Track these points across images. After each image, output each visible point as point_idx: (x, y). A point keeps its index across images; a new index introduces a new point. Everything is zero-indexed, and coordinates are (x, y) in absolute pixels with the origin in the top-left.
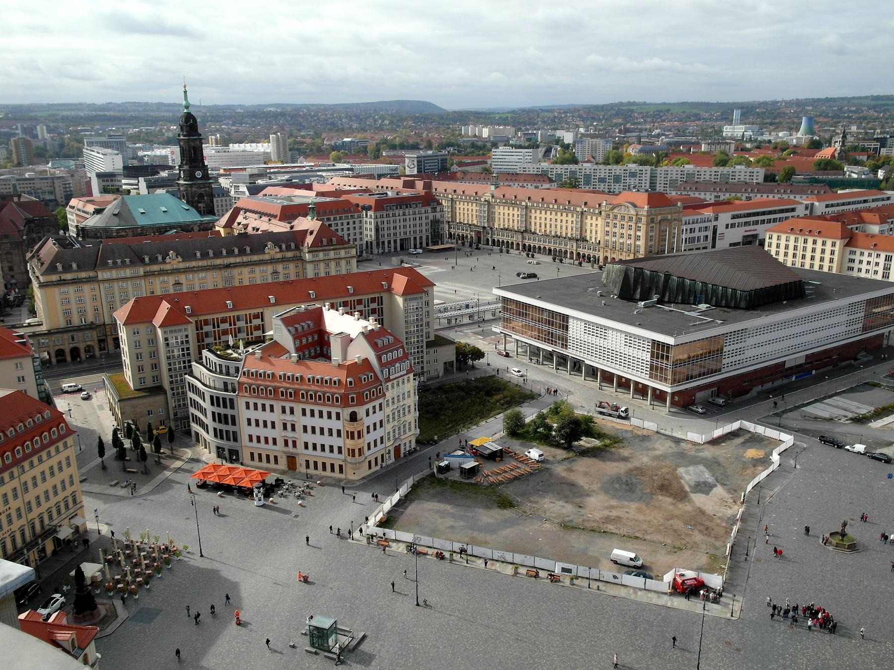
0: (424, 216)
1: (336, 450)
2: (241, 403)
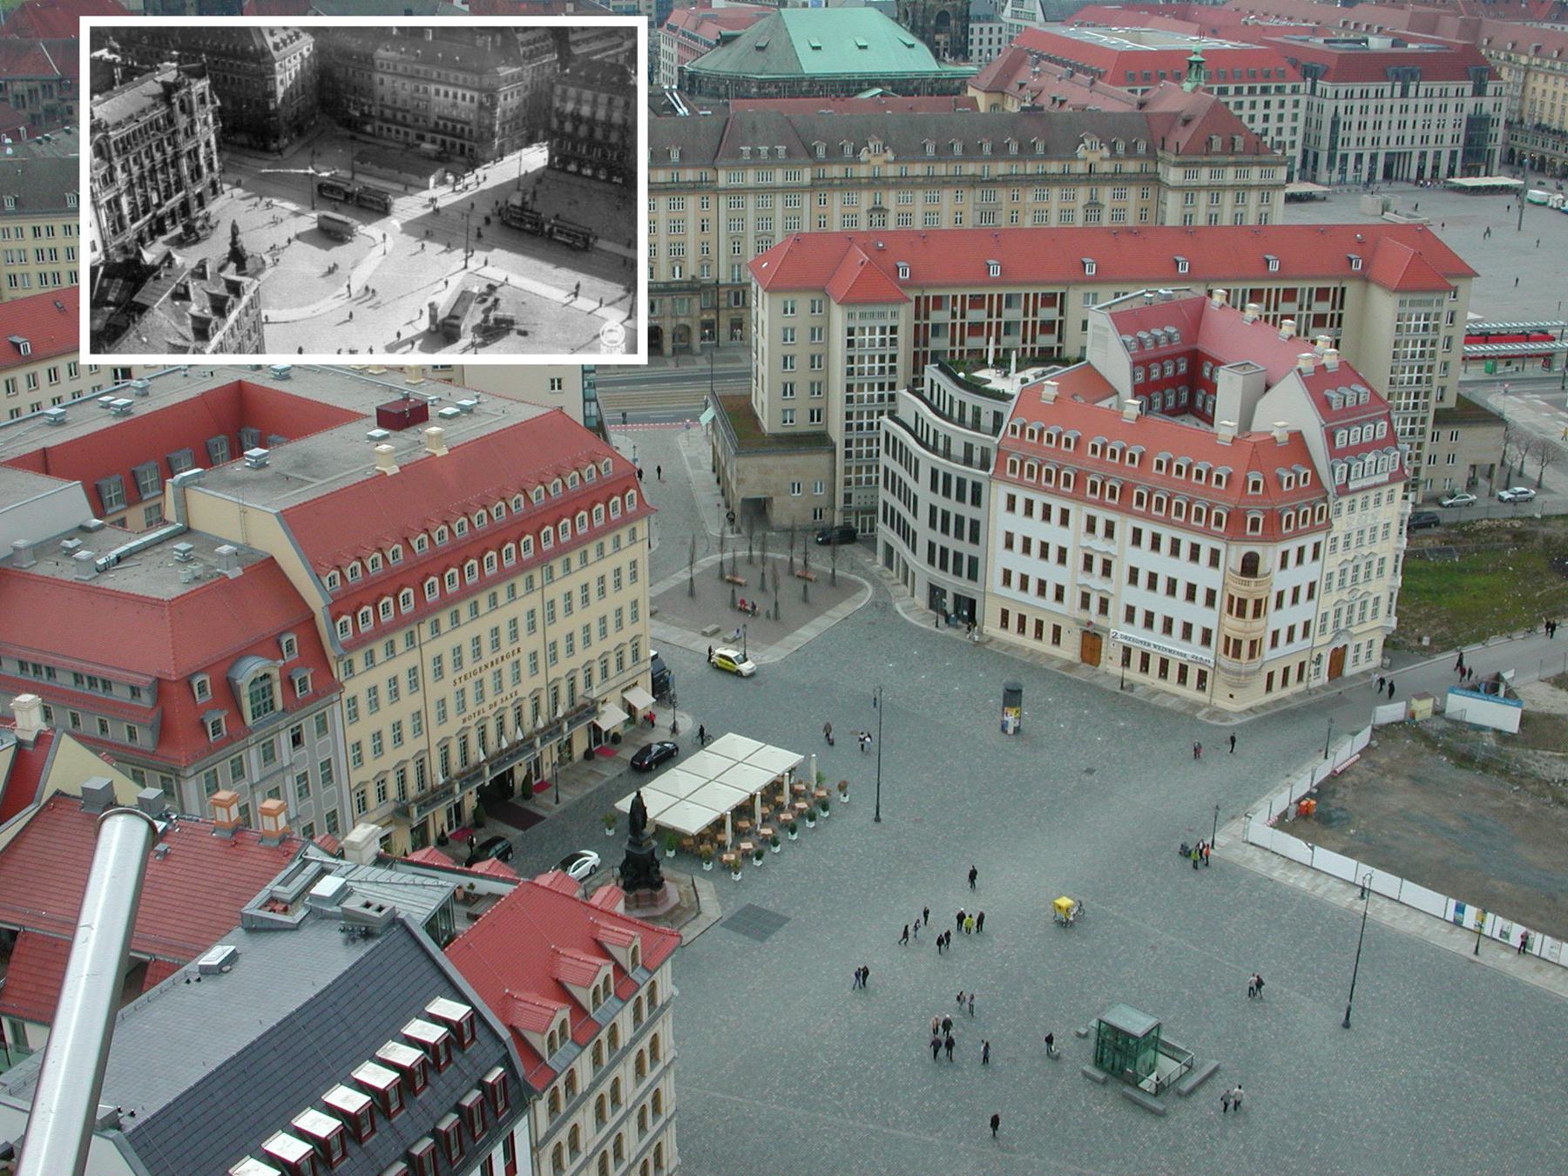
2: (997, 494)
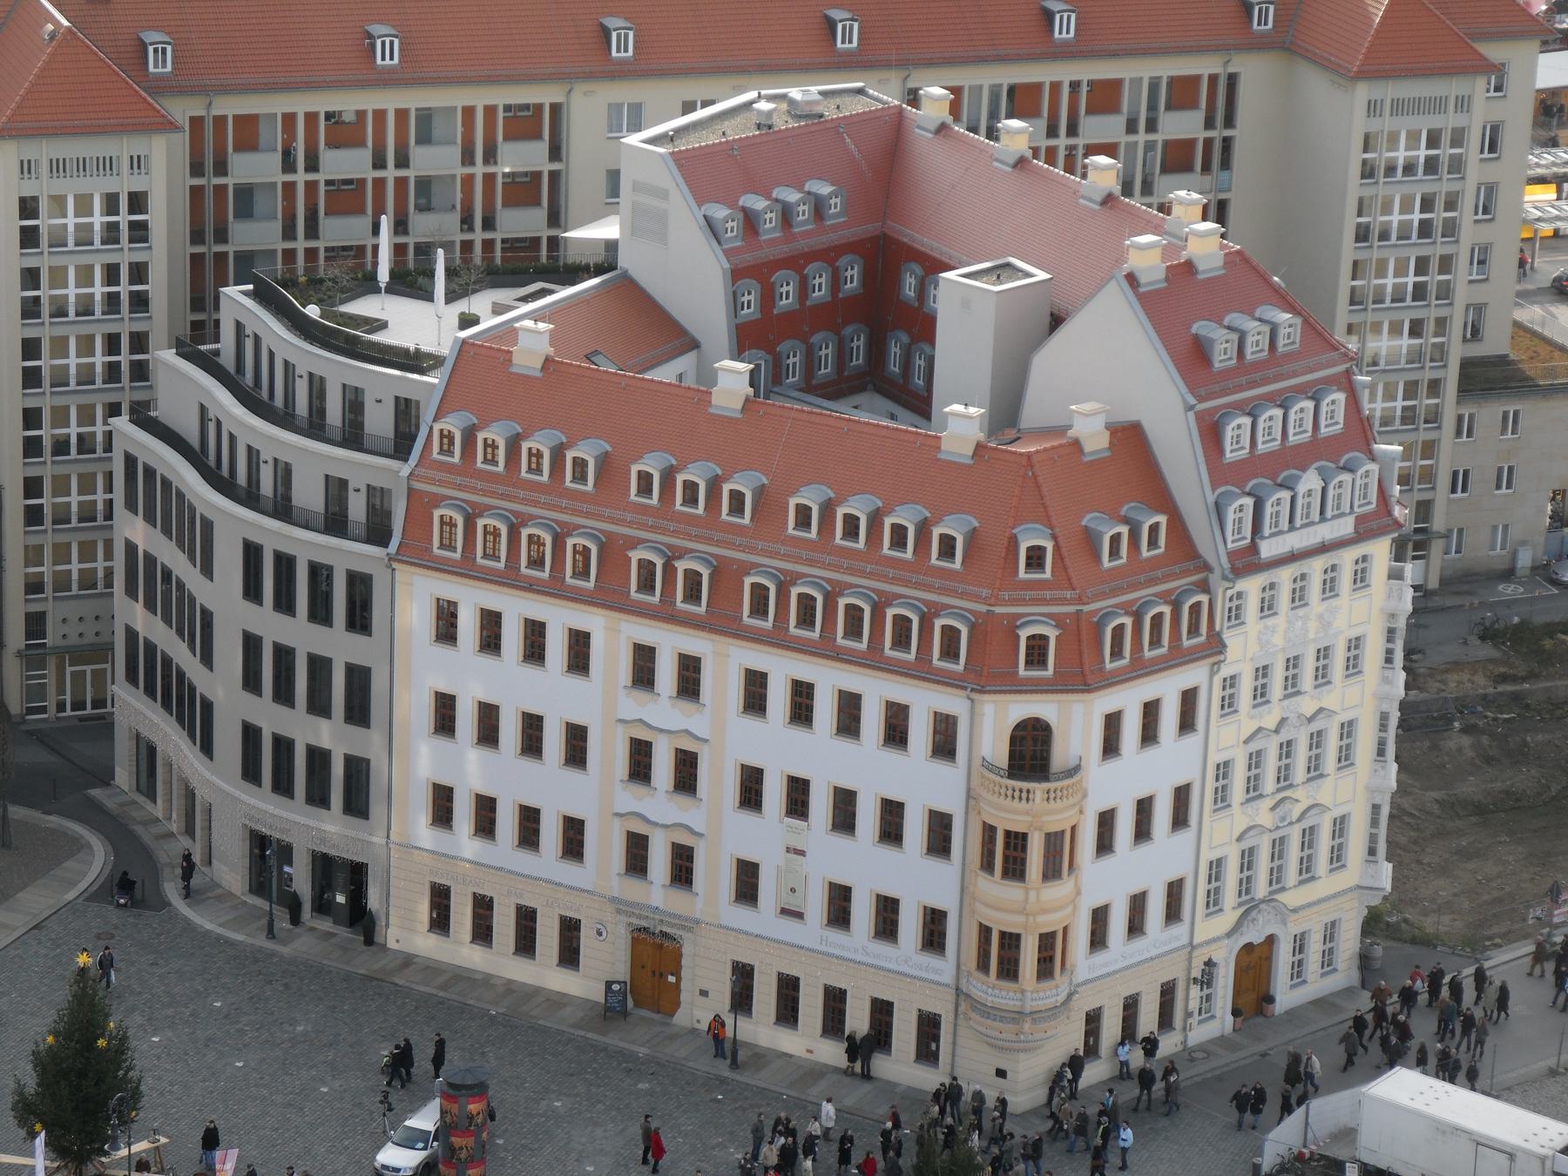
1: (910, 925)
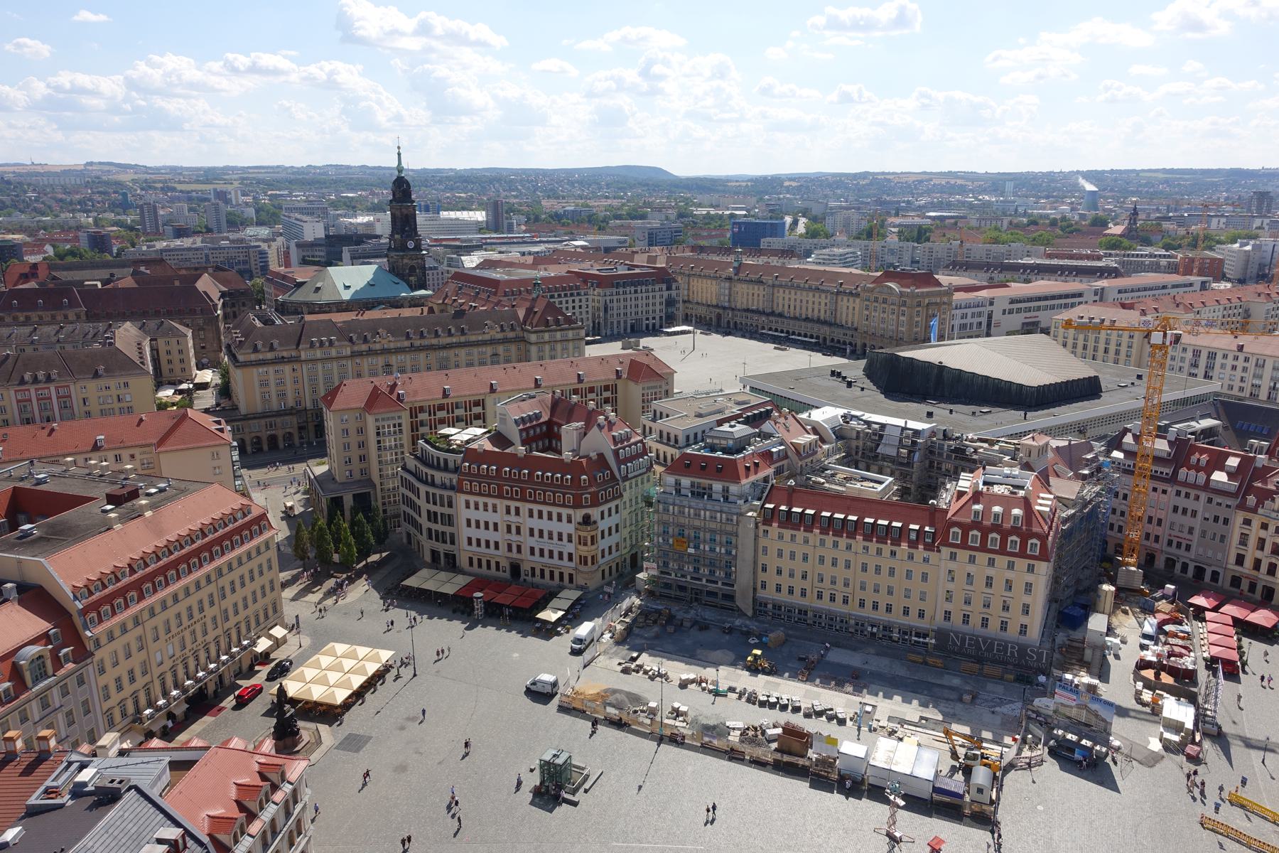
0: (658, 294)
1: (566, 556)
